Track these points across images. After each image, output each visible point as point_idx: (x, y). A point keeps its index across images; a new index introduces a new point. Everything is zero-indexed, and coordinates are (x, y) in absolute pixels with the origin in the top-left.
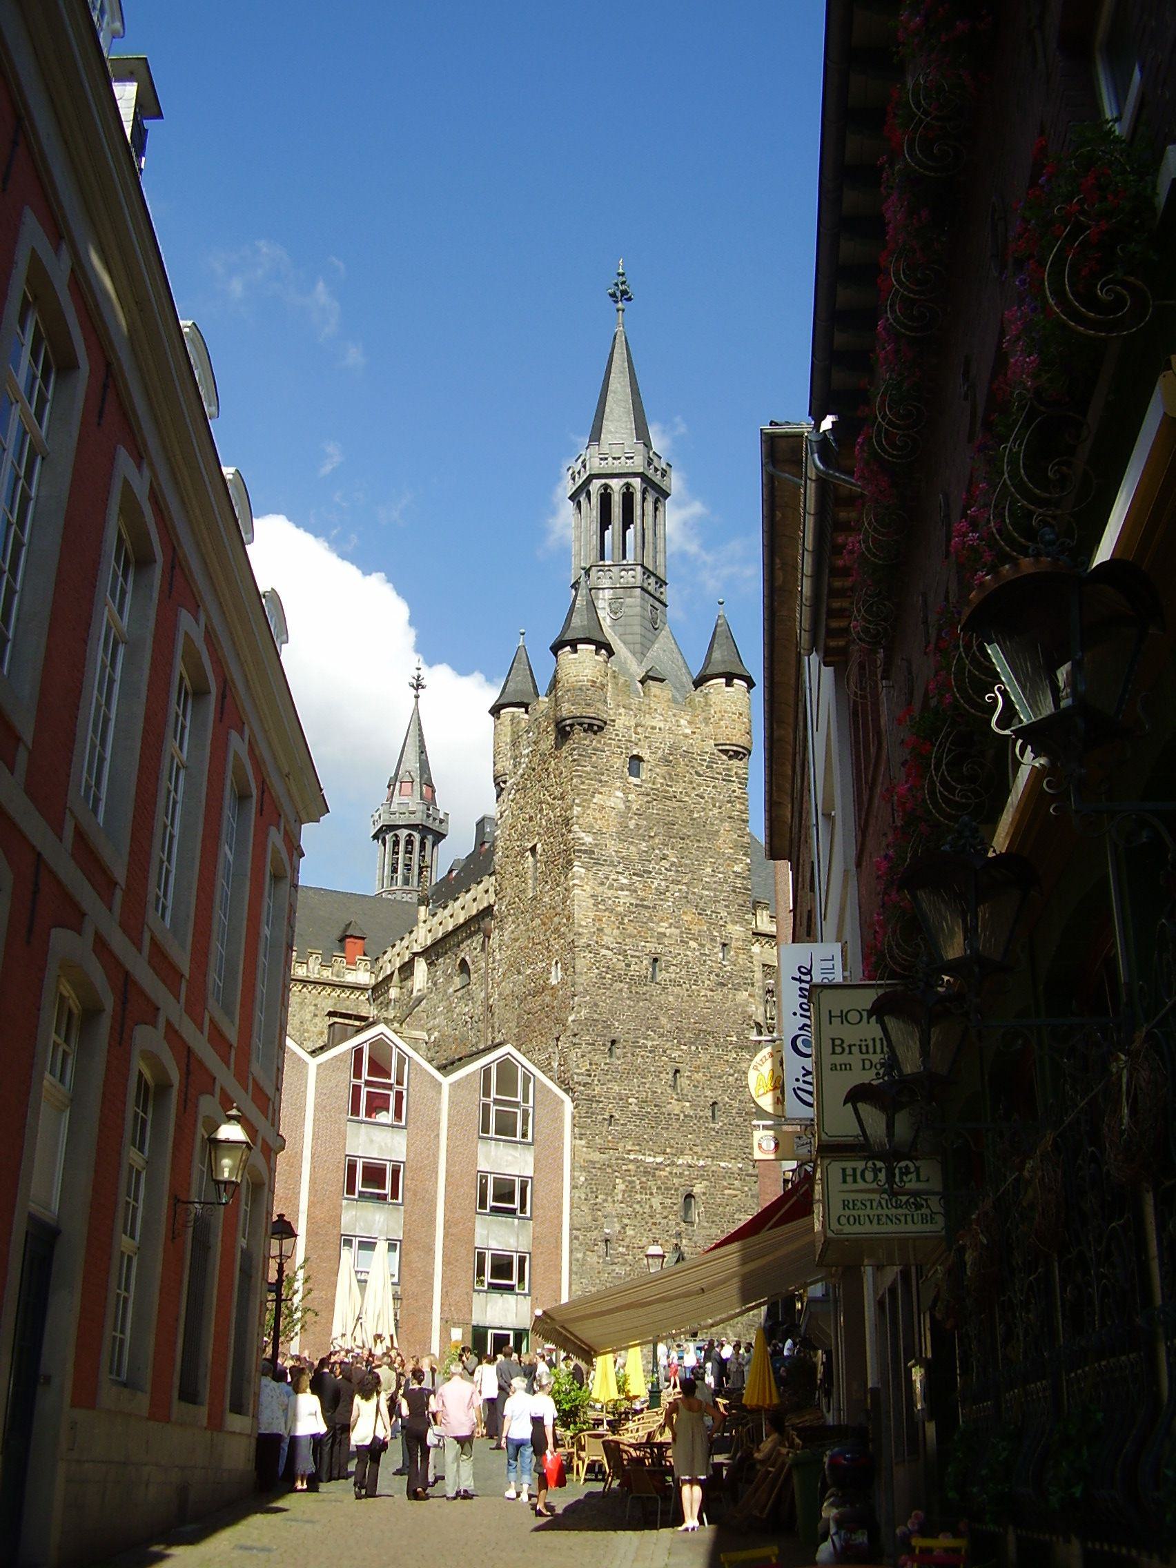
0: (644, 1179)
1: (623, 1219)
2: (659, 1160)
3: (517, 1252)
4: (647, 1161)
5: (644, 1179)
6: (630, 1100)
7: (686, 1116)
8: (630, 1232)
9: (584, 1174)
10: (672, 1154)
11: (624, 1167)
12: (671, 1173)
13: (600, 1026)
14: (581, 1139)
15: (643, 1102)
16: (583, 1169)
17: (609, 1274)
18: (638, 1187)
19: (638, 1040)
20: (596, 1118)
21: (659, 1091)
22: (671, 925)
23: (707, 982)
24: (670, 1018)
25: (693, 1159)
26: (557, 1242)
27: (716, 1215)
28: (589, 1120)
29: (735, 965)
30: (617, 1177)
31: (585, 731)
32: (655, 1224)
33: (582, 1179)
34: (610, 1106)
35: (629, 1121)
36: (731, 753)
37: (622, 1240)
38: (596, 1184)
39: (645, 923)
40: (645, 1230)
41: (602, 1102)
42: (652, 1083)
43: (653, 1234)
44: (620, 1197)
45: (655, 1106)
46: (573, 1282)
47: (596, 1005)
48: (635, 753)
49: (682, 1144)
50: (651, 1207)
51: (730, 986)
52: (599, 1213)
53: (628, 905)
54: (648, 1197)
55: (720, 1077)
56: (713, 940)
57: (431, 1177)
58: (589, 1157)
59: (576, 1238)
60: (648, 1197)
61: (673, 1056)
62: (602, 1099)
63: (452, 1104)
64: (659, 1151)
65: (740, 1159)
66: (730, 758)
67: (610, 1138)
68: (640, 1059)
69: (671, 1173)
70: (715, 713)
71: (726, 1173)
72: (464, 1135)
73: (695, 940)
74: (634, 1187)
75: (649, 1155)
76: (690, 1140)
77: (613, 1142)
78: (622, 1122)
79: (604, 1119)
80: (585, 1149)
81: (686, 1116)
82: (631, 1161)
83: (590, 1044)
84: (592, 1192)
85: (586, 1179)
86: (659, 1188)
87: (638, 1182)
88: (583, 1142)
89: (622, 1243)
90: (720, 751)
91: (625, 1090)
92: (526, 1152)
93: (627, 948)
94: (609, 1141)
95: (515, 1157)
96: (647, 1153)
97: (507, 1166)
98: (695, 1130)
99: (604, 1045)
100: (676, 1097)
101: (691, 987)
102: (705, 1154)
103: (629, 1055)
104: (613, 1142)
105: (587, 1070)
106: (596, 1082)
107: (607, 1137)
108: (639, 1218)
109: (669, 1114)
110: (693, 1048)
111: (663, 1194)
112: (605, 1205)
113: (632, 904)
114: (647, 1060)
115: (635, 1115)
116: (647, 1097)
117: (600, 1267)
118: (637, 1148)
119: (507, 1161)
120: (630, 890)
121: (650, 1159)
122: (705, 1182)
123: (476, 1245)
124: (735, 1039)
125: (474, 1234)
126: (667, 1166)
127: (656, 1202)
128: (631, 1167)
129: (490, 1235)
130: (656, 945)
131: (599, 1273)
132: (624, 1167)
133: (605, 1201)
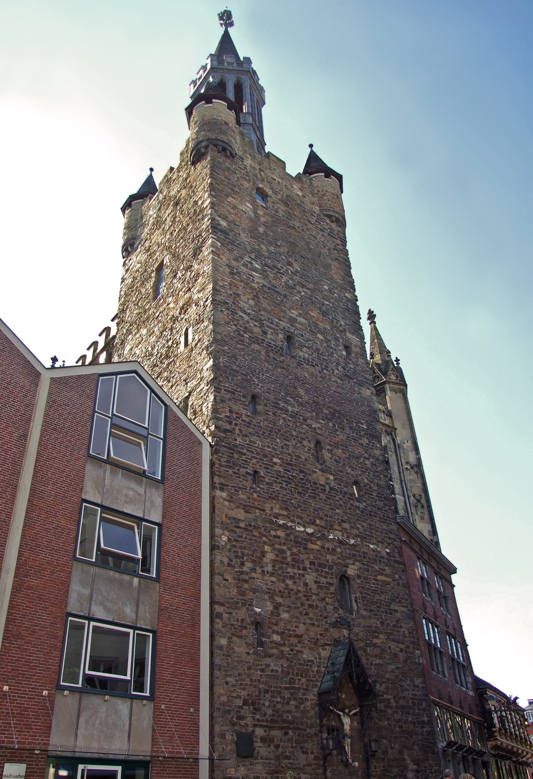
0: (295, 550)
1: (276, 598)
2: (310, 530)
3: (134, 628)
4: (297, 529)
5: (295, 550)
6: (275, 460)
7: (331, 488)
8: (285, 616)
9: (227, 533)
10: (322, 527)
11: (273, 533)
13: (239, 378)
14: (222, 490)
15: (287, 465)
16: (224, 526)
17: (262, 670)
18: (289, 559)
19: (280, 402)
20: (238, 470)
21: (303, 457)
22: (300, 315)
23: (336, 372)
24: (307, 391)
25: (343, 535)
27: (373, 602)
28: (231, 472)
29: (357, 365)
30: (265, 543)
31: (219, 152)
32: (311, 606)
33: (225, 538)
34: (254, 461)
35: (276, 482)
36: (334, 219)
37: (276, 625)
38: (241, 547)
39: (278, 304)
40: (301, 613)
41: (245, 454)
42: (295, 447)
44: (269, 568)
45: (301, 471)
46: (217, 681)
47: (234, 356)
48: (260, 186)
49: (331, 517)
50: (306, 584)
51: (355, 380)
52: (246, 586)
53: (261, 284)
54: (301, 572)
55: (358, 458)
56: (336, 339)
57: (5, 492)
58: (232, 514)
59: (219, 616)
60: (301, 572)
61: (313, 426)
62: (245, 451)
63: (51, 403)
64: (308, 520)
65: (386, 544)
66: (332, 222)
67: (255, 495)
68: (281, 421)
69: (323, 547)
70: (318, 191)
71: (376, 556)
72: (67, 447)
73: (322, 334)
74: (286, 558)
75: (299, 523)
76: (338, 514)
77: (259, 501)
78: (267, 480)
79: (247, 473)
80: (226, 503)
81: (331, 488)
82: (280, 526)
83: (229, 392)
84: (237, 557)
85: (229, 540)
86: (312, 563)
87: (289, 553)
88: (224, 495)
89: (276, 628)
90: (324, 215)
91: (268, 447)
92: (154, 490)
93: (263, 318)
94: (254, 499)
95: (139, 494)
96: (297, 521)
97: (126, 502)
98: (341, 506)
99: (244, 397)
100: (320, 467)
101: (322, 370)
102: (355, 532)
103: (271, 414)
104: (259, 501)
105: (226, 416)
106: (237, 431)
107: (252, 494)
108: (293, 597)
109: (315, 483)
110: (331, 424)
111: (317, 571)
112: (253, 575)
113: (264, 286)
114: (289, 423)
115: (280, 476)
116: (291, 460)
117: (251, 659)
118: (285, 513)
119: (126, 496)
120: (262, 274)
121: (302, 529)
122: (357, 564)
123: (70, 610)
124: (365, 427)
125: (67, 591)
126: (319, 538)
127: (310, 578)
128: (280, 533)
129: (95, 595)
130: (290, 326)
131: (249, 668)
132: (273, 533)
133: (253, 570)
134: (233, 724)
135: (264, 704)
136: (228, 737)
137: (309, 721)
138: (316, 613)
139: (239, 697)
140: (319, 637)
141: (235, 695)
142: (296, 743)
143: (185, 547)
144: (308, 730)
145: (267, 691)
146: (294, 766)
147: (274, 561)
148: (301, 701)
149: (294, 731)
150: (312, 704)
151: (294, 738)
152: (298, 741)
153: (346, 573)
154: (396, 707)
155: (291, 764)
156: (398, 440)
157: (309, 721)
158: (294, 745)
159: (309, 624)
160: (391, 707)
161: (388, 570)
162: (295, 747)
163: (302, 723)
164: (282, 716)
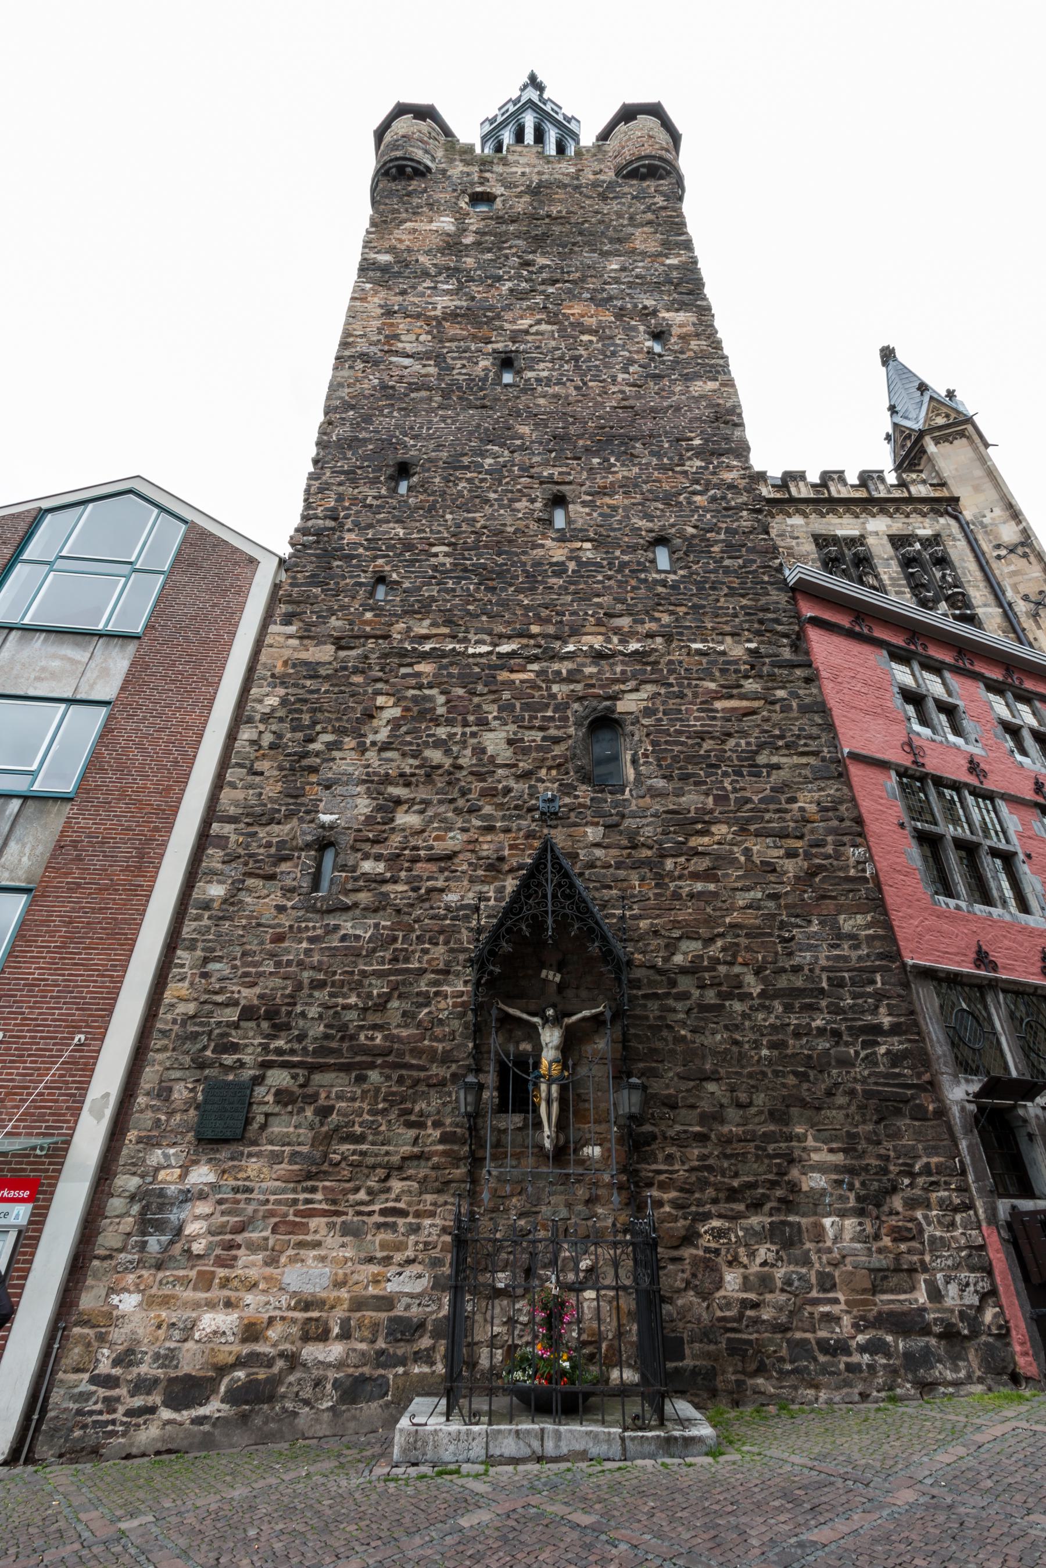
12: (538, 674)
18: (441, 711)
26: (141, 855)
37: (375, 842)
43: (483, 818)
81: (580, 563)
128: (425, 668)
131: (279, 938)
133: (335, 746)
134: (201, 1065)
135: (303, 1014)
136: (180, 1093)
137: (440, 1047)
138: (502, 804)
139: (233, 1003)
140: (506, 853)
141: (219, 999)
142: (385, 1100)
143: (160, 730)
144: (435, 1070)
145: (321, 985)
146: (371, 1160)
147: (395, 724)
148: (421, 1000)
149: (387, 1071)
150: (455, 1005)
151: (383, 1090)
152: (393, 1094)
153: (613, 711)
154: (763, 994)
155: (363, 1154)
156: (968, 514)
157: (440, 1047)
158: (380, 1106)
159: (479, 828)
160: (744, 997)
161: (751, 685)
162: (384, 1112)
163: (418, 1052)
164: (353, 1037)
